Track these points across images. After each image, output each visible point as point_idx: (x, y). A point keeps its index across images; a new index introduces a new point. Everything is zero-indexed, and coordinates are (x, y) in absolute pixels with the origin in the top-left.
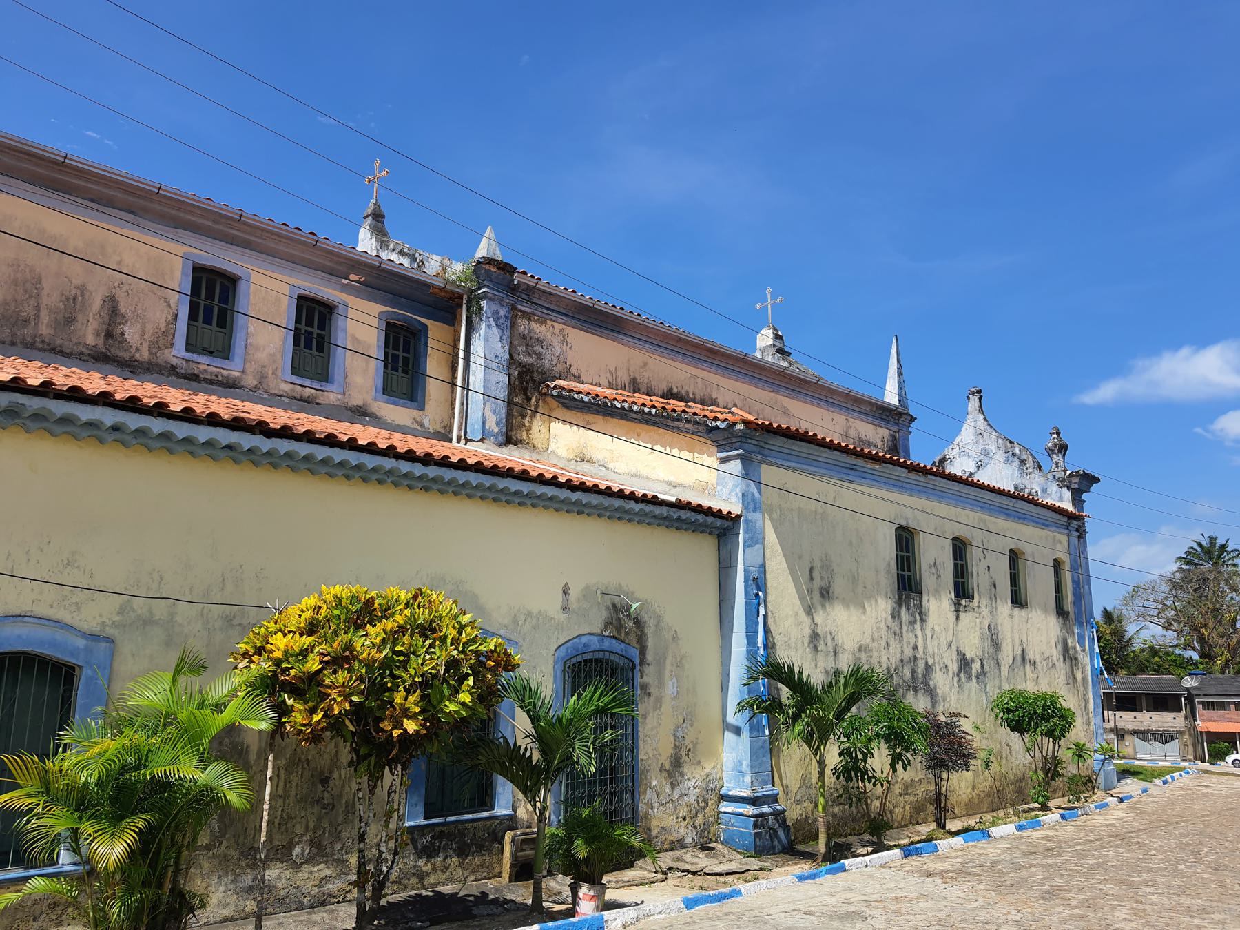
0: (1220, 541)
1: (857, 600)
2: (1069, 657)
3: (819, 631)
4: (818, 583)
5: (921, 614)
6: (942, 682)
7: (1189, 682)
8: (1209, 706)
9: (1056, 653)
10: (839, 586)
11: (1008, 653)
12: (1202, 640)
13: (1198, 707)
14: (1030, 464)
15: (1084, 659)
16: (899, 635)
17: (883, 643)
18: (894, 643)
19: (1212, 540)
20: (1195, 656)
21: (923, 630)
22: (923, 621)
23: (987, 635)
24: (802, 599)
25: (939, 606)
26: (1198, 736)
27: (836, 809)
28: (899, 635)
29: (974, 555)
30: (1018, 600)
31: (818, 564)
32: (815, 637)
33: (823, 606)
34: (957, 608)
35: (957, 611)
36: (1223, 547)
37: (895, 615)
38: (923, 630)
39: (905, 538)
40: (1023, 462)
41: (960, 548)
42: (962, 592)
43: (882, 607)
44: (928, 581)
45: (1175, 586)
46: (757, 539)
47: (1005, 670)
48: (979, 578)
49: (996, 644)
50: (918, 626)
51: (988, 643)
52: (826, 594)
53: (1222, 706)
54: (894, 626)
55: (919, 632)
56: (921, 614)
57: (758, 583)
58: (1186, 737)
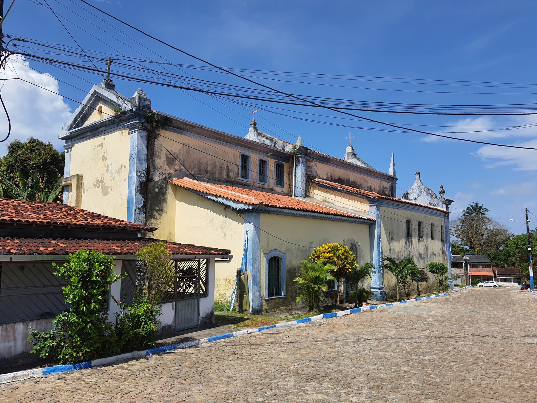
0: (480, 205)
1: (398, 240)
2: (444, 253)
3: (391, 248)
4: (391, 236)
5: (411, 242)
6: (415, 260)
7: (466, 258)
8: (473, 266)
9: (440, 252)
10: (395, 237)
11: (430, 252)
12: (471, 242)
13: (469, 266)
14: (434, 196)
15: (447, 253)
16: (407, 248)
17: (403, 250)
18: (406, 251)
19: (477, 204)
20: (468, 247)
21: (412, 247)
22: (412, 244)
23: (425, 248)
24: (388, 240)
25: (415, 240)
26: (468, 277)
27: (394, 291)
28: (407, 248)
29: (423, 225)
30: (432, 238)
31: (391, 231)
32: (390, 249)
33: (392, 242)
34: (419, 240)
35: (419, 241)
36: (481, 207)
37: (406, 243)
38: (412, 247)
39: (408, 222)
40: (432, 195)
41: (420, 223)
42: (420, 236)
43: (403, 241)
44: (413, 234)
45: (462, 221)
46: (379, 226)
47: (429, 256)
48: (424, 233)
49: (427, 250)
50: (410, 246)
51: (425, 250)
52: (392, 239)
53: (477, 266)
54: (406, 246)
55: (411, 247)
56: (411, 242)
57: (379, 237)
58: (464, 277)
